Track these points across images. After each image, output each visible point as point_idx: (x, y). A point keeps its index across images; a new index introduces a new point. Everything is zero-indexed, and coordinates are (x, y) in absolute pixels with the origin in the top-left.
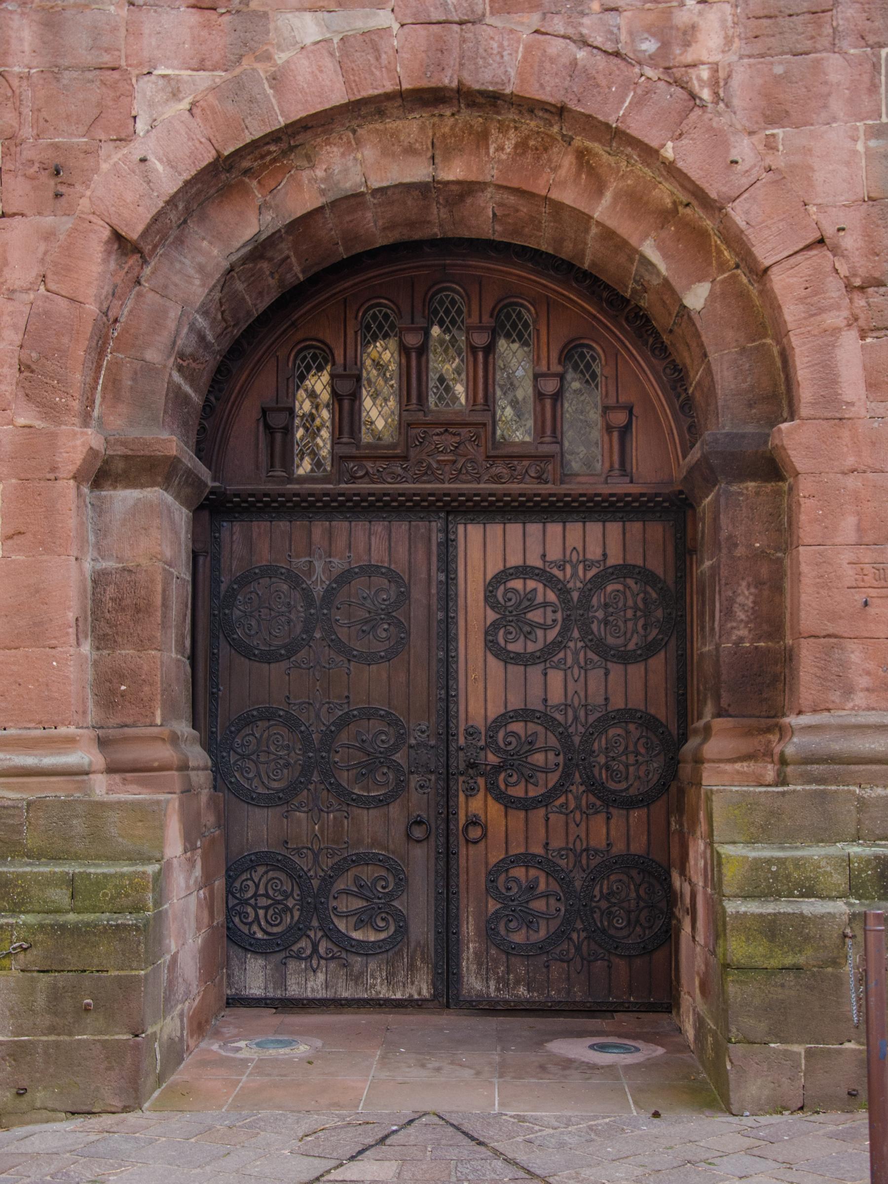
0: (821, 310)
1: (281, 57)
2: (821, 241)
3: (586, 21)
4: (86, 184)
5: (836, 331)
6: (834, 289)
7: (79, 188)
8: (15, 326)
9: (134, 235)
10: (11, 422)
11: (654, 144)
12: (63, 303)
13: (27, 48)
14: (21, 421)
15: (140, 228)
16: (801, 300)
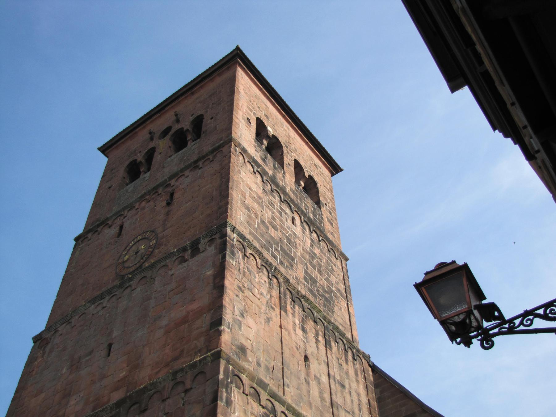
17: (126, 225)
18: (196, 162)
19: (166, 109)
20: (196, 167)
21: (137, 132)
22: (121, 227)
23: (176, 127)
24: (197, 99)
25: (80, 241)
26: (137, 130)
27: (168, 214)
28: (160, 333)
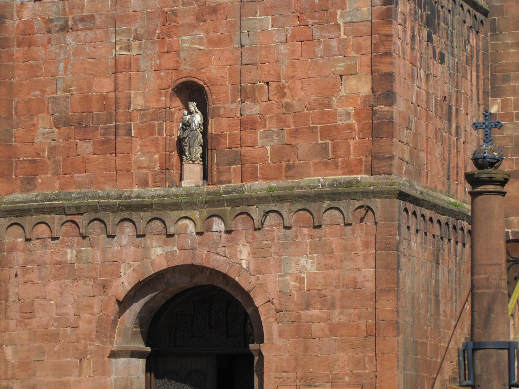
0: (269, 317)
1: (153, 257)
2: (269, 301)
3: (219, 249)
4: (111, 288)
5: (272, 323)
6: (272, 312)
7: (109, 289)
8: (95, 322)
9: (121, 300)
10: (94, 345)
11: (233, 278)
12: (105, 317)
13: (98, 257)
14: (96, 344)
15: (122, 299)
16: (265, 315)
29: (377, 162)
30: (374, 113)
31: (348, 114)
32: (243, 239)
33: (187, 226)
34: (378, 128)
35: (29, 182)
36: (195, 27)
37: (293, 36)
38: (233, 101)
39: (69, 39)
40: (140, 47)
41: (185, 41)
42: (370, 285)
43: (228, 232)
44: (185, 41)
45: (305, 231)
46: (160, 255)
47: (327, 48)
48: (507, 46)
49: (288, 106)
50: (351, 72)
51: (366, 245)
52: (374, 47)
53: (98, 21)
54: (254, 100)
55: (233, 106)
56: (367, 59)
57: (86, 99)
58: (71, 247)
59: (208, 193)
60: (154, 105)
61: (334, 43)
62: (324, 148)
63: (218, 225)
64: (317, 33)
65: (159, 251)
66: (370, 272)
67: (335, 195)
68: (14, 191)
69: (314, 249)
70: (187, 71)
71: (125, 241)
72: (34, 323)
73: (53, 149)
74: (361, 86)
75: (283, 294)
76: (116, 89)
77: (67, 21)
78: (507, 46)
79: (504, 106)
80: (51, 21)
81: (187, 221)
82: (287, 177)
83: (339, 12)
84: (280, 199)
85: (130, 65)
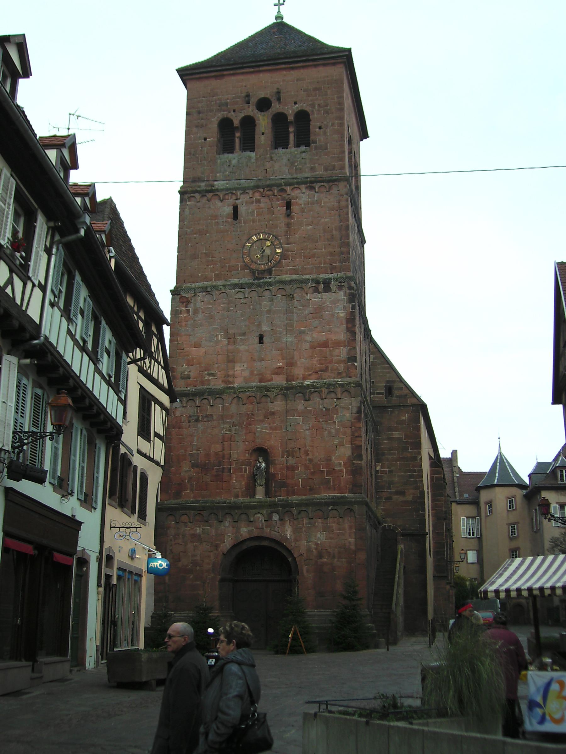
17: (242, 210)
18: (312, 182)
19: (261, 69)
20: (312, 188)
21: (223, 76)
22: (235, 209)
23: (276, 107)
24: (298, 80)
25: (186, 196)
26: (225, 73)
27: (288, 225)
28: (306, 346)
29: (355, 487)
30: (354, 464)
31: (340, 464)
32: (287, 524)
33: (259, 518)
34: (356, 472)
35: (178, 495)
36: (263, 421)
37: (313, 427)
38: (283, 457)
39: (200, 425)
40: (235, 430)
41: (258, 428)
42: (353, 547)
43: (281, 520)
44: (258, 428)
45: (320, 520)
46: (245, 531)
47: (330, 432)
48: (384, 439)
49: (311, 460)
50: (341, 444)
51: (351, 528)
52: (353, 433)
53: (215, 418)
54: (293, 456)
55: (282, 459)
56: (349, 439)
57: (208, 455)
58: (199, 527)
59: (270, 501)
60: (242, 458)
61: (333, 431)
62: (328, 481)
63: (276, 517)
64: (324, 426)
65: (245, 529)
66: (352, 541)
67: (335, 503)
68: (170, 499)
69: (324, 529)
70: (259, 442)
71: (227, 524)
72: (180, 564)
73: (190, 479)
74: (346, 451)
75: (309, 550)
76: (223, 450)
77: (198, 417)
78: (384, 439)
79: (382, 466)
80: (191, 417)
81: (259, 515)
82: (310, 494)
83: (335, 416)
84: (307, 505)
85: (231, 438)
